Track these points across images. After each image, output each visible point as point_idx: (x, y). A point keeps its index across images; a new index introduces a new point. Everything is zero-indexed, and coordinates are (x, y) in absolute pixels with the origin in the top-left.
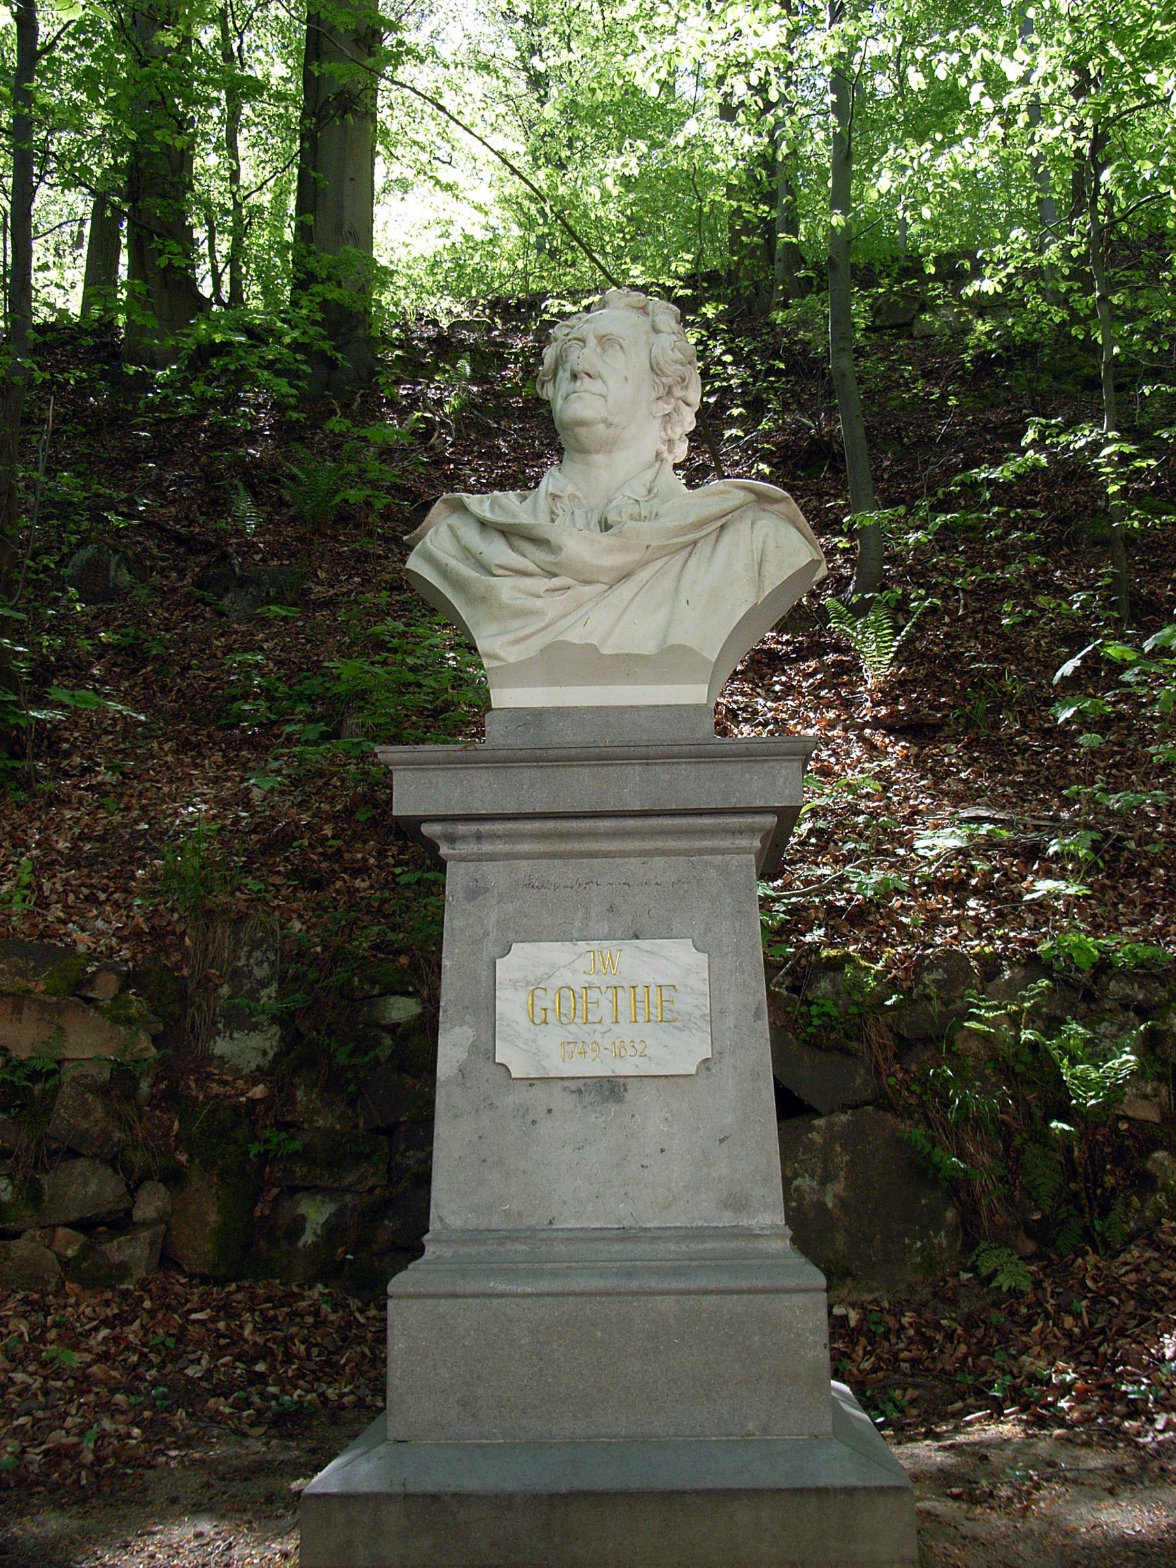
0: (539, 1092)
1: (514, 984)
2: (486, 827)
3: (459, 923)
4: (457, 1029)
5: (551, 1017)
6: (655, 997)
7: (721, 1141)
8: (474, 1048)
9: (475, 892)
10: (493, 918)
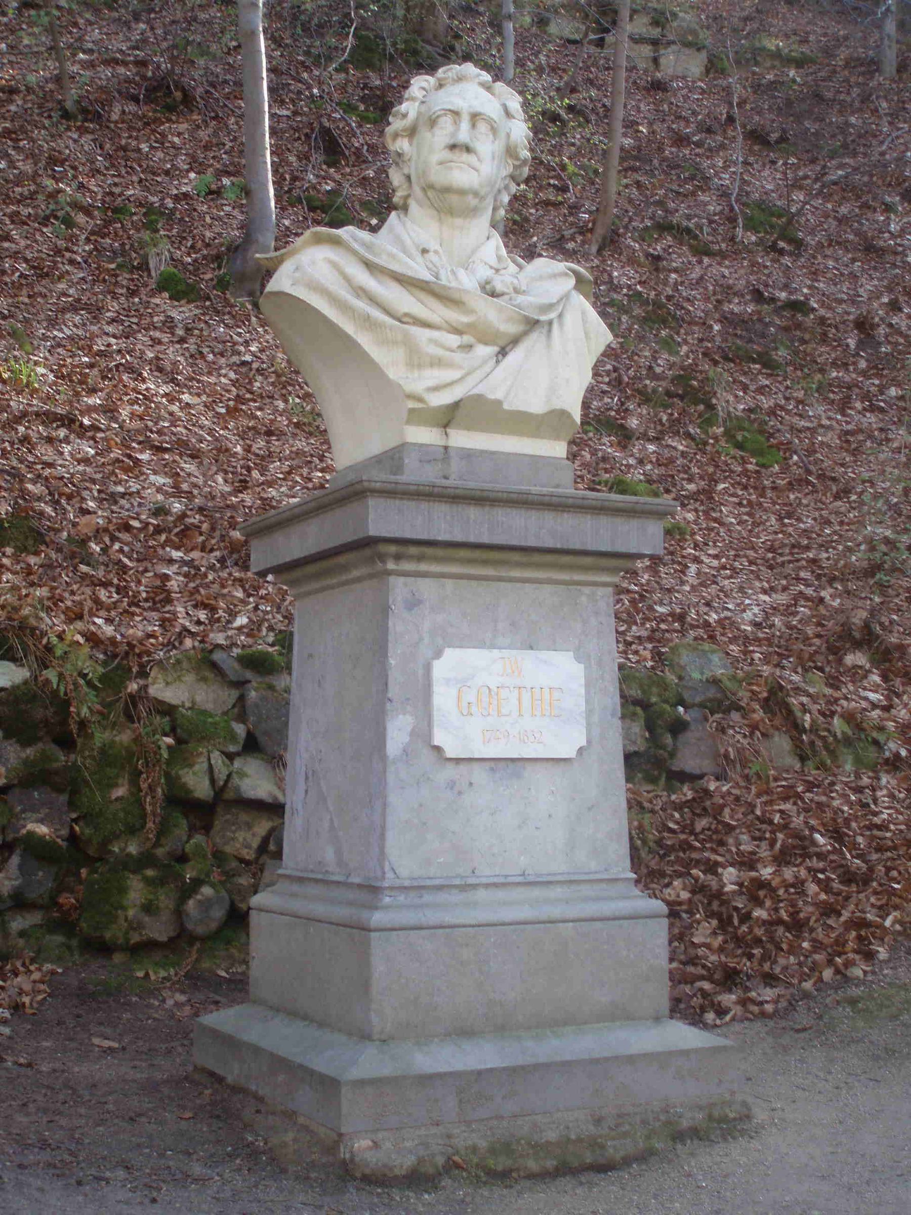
0: (463, 767)
1: (448, 681)
2: (429, 551)
3: (400, 628)
4: (401, 716)
5: (474, 709)
6: (547, 696)
7: (590, 809)
8: (413, 733)
9: (413, 603)
10: (427, 625)
